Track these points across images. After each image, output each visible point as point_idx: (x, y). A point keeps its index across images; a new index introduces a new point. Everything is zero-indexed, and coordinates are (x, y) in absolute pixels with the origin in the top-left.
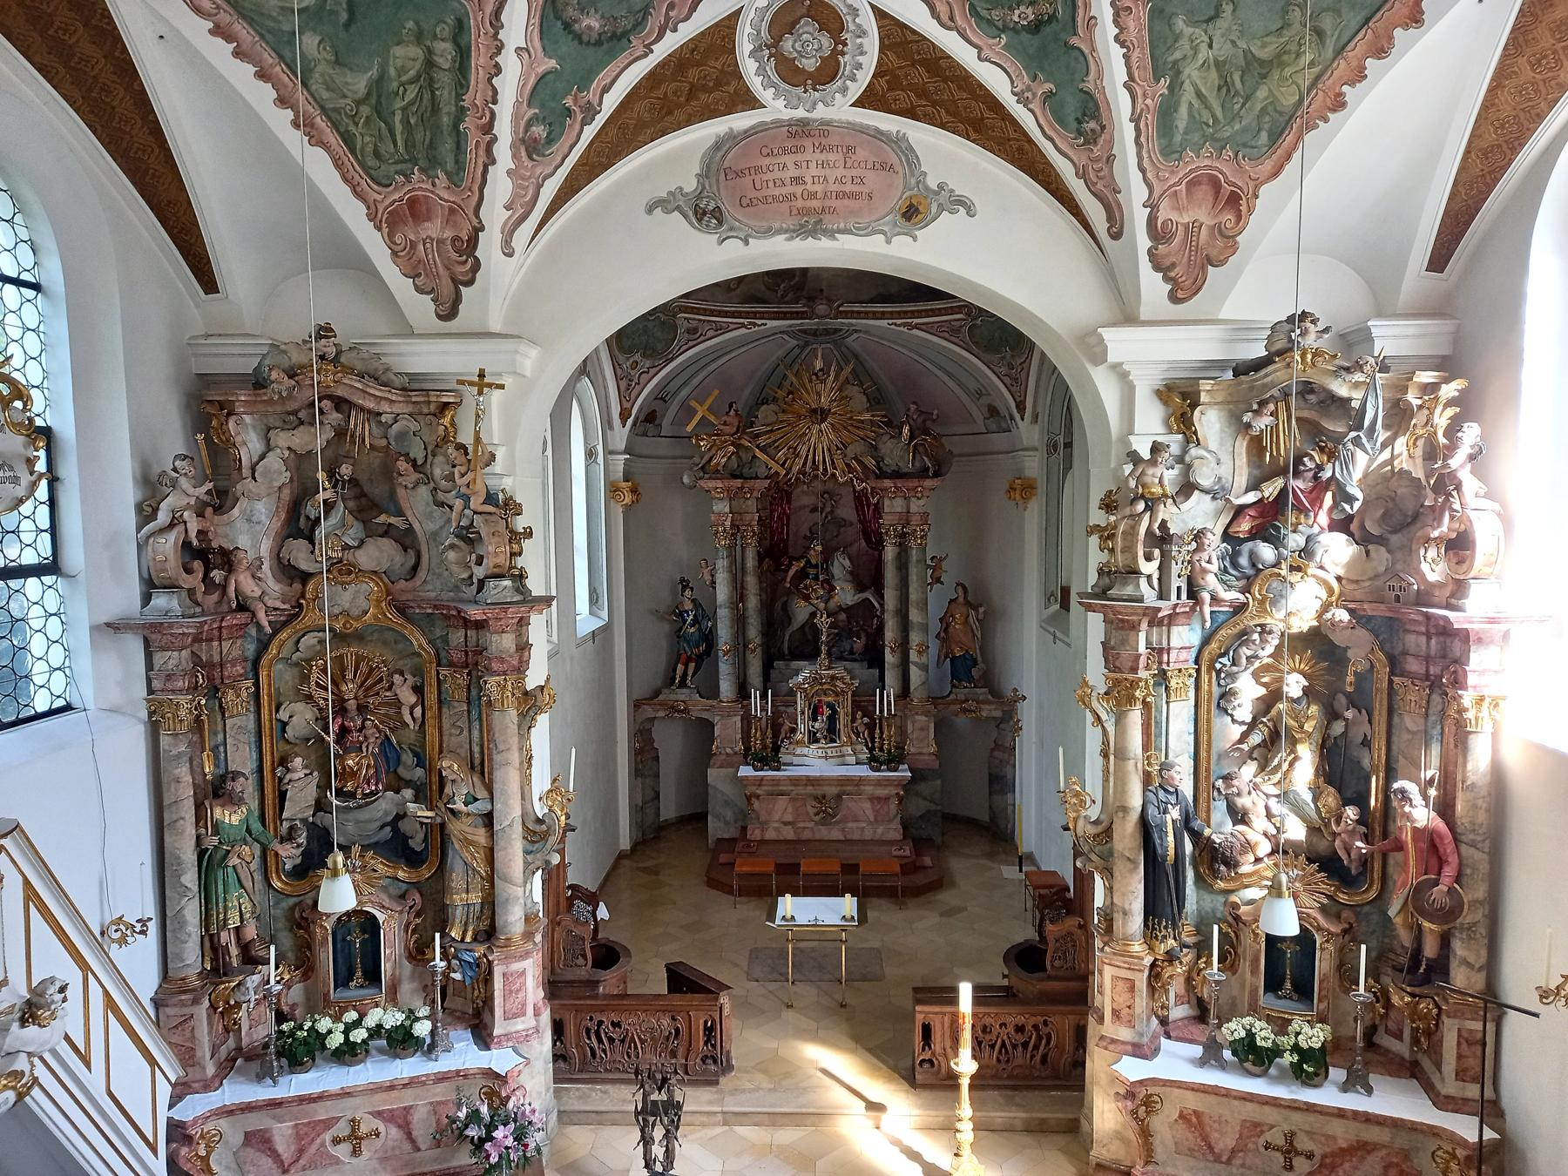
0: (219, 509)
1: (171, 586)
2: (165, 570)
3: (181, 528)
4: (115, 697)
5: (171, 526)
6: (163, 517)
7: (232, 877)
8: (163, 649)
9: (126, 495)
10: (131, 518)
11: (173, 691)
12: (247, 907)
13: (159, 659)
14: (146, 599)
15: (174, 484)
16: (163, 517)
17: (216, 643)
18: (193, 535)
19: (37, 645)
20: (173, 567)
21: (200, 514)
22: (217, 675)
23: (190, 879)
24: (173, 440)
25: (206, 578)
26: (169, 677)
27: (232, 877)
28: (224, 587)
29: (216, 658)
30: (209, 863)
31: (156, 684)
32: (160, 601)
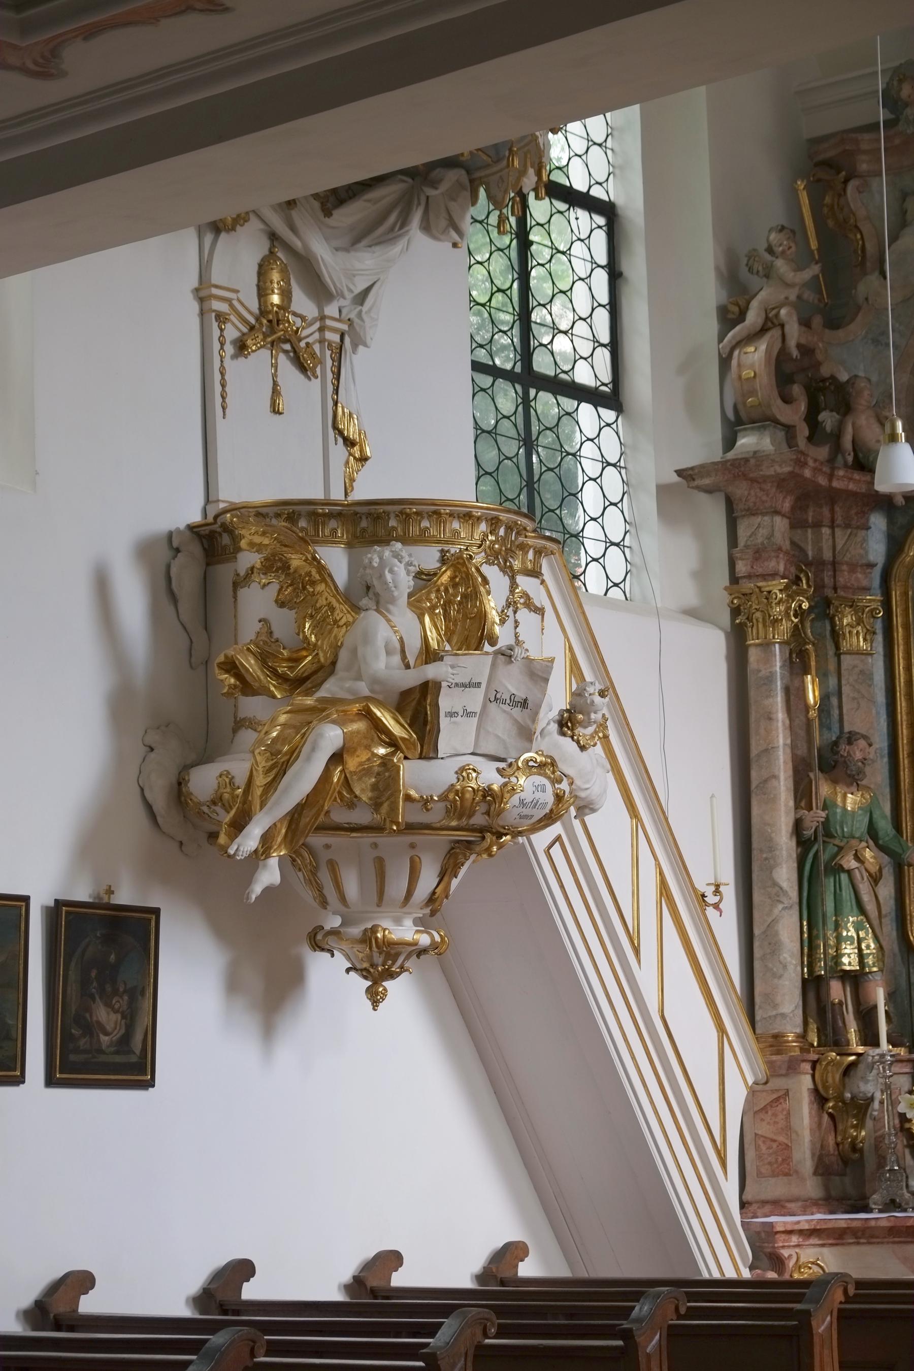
0: (834, 323)
1: (763, 420)
2: (753, 393)
3: (776, 333)
4: (691, 598)
5: (763, 330)
6: (753, 317)
7: (847, 894)
8: (752, 512)
9: (708, 293)
10: (713, 325)
11: (765, 577)
12: (870, 947)
13: (743, 533)
14: (729, 442)
15: (768, 273)
16: (753, 317)
17: (826, 531)
18: (792, 343)
19: (590, 497)
20: (765, 384)
21: (806, 323)
22: (828, 581)
23: (785, 874)
24: (770, 203)
25: (812, 419)
26: (758, 554)
27: (847, 894)
28: (836, 437)
29: (827, 555)
30: (816, 850)
31: (742, 568)
32: (747, 442)
